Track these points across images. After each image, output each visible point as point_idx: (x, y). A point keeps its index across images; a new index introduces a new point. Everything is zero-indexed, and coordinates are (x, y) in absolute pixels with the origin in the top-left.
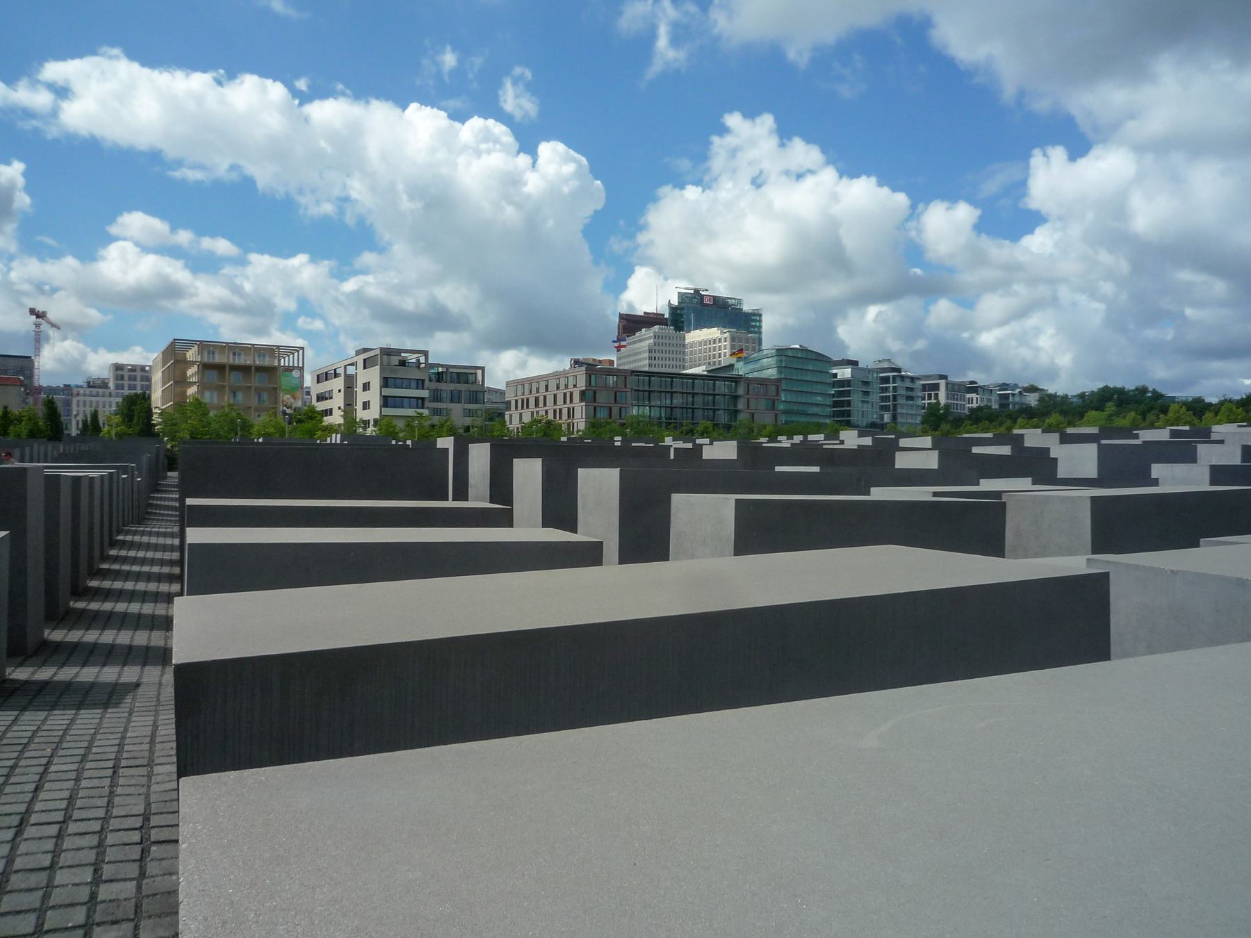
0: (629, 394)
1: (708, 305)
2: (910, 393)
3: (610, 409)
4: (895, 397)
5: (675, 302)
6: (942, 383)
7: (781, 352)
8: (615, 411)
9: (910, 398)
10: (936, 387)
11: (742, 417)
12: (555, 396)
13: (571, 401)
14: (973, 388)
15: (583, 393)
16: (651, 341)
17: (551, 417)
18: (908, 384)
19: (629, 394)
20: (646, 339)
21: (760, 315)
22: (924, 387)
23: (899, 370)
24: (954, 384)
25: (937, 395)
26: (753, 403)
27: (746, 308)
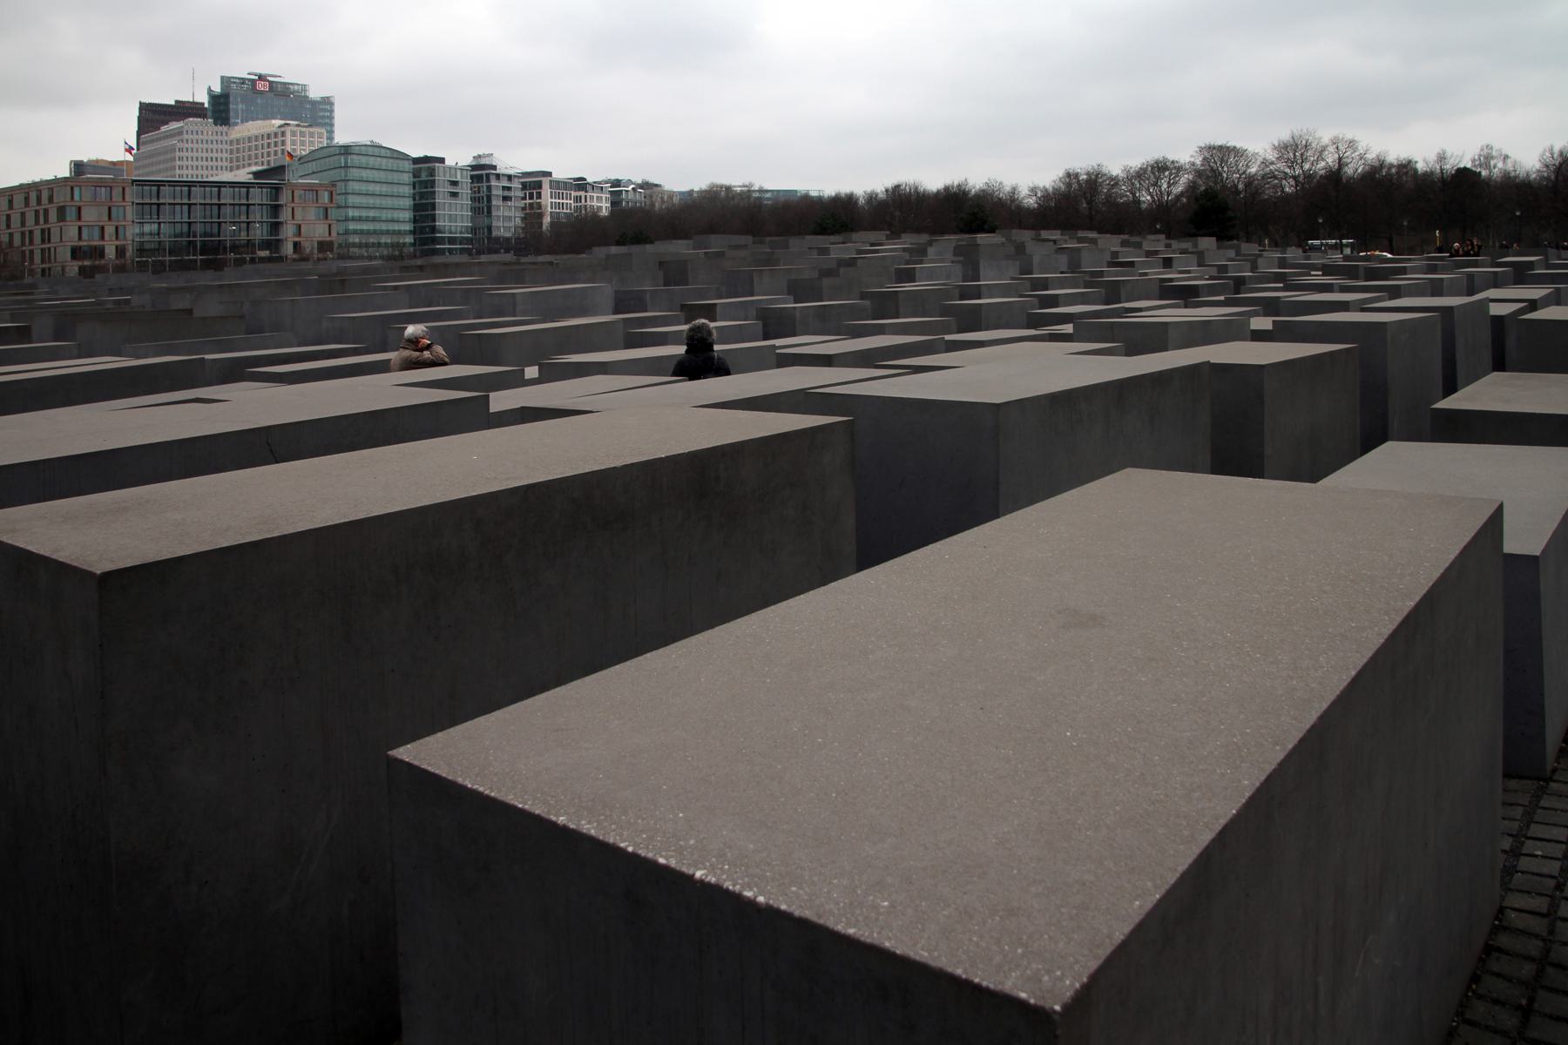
0: (129, 210)
2: (506, 193)
3: (102, 228)
4: (489, 198)
5: (217, 89)
6: (546, 182)
8: (110, 230)
9: (505, 199)
10: (539, 185)
11: (288, 232)
12: (23, 214)
13: (46, 221)
14: (580, 184)
15: (62, 211)
17: (17, 241)
19: (129, 210)
23: (494, 167)
24: (558, 182)
25: (539, 196)
26: (298, 213)
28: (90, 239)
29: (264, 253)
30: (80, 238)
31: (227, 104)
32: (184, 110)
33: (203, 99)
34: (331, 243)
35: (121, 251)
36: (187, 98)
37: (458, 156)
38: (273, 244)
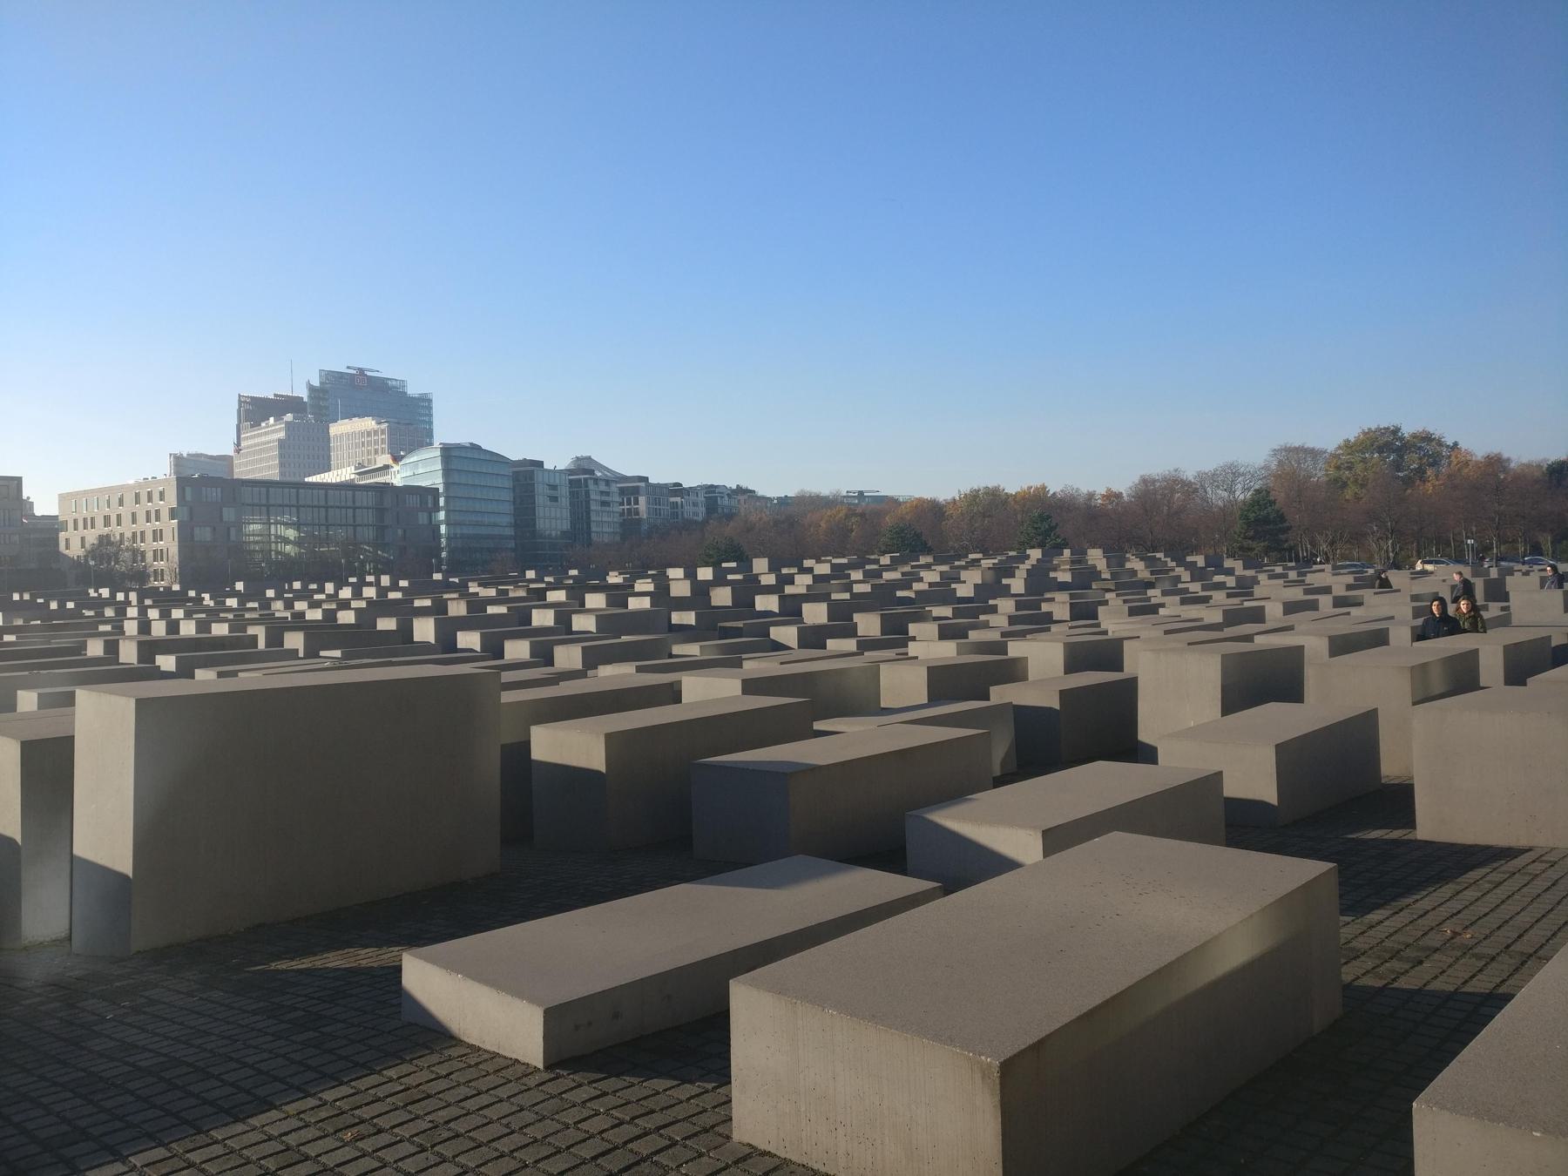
2: (604, 498)
5: (316, 383)
7: (449, 452)
9: (604, 504)
14: (677, 490)
16: (282, 435)
18: (603, 487)
20: (274, 431)
21: (430, 401)
22: (622, 491)
25: (637, 502)
27: (413, 390)
33: (303, 394)
37: (557, 459)
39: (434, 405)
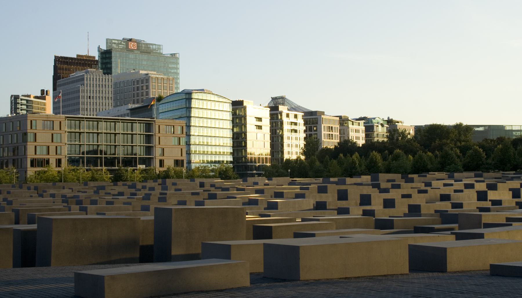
1: (132, 51)
2: (294, 127)
5: (104, 47)
21: (178, 59)
27: (166, 51)
28: (41, 155)
29: (143, 167)
30: (36, 154)
31: (110, 58)
32: (83, 62)
33: (96, 55)
34: (183, 161)
35: (59, 162)
36: (84, 53)
38: (147, 161)
39: (181, 61)
